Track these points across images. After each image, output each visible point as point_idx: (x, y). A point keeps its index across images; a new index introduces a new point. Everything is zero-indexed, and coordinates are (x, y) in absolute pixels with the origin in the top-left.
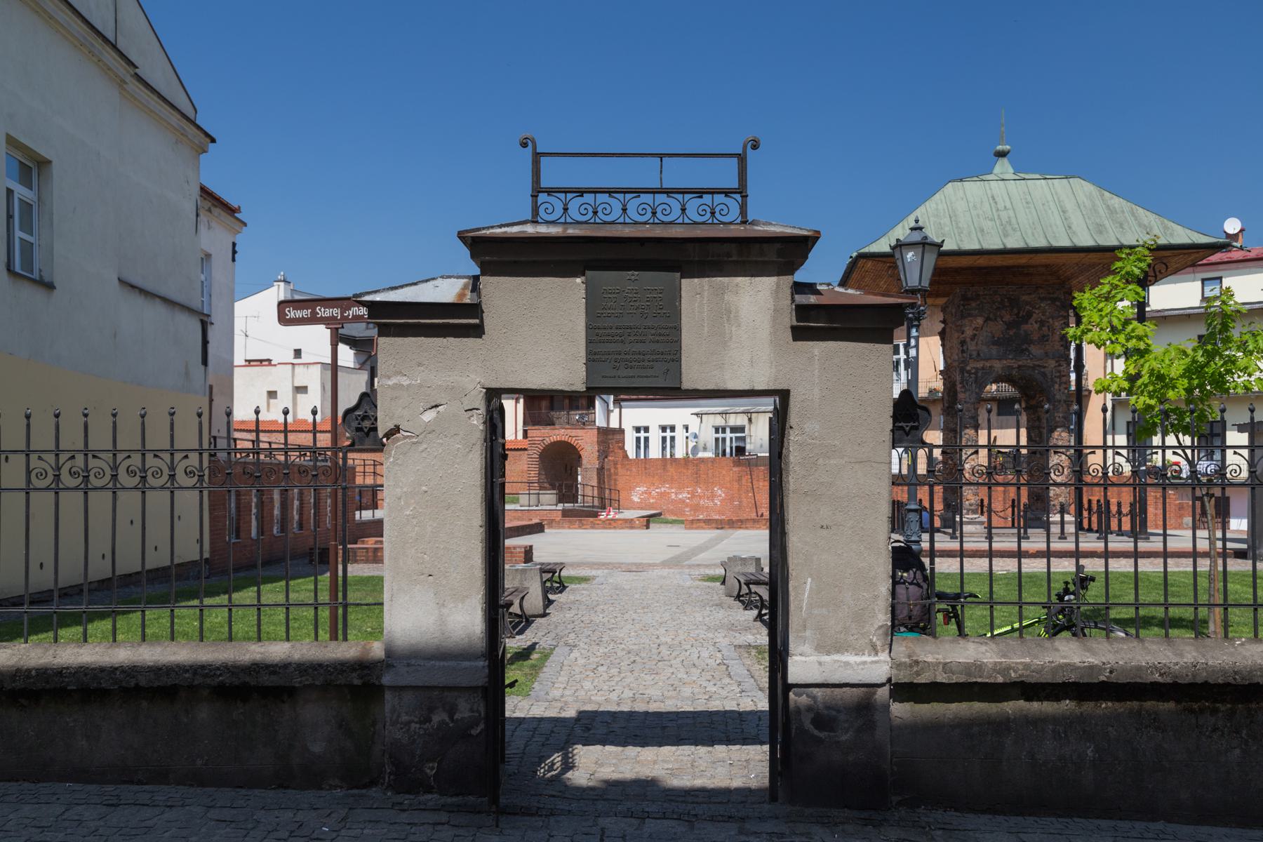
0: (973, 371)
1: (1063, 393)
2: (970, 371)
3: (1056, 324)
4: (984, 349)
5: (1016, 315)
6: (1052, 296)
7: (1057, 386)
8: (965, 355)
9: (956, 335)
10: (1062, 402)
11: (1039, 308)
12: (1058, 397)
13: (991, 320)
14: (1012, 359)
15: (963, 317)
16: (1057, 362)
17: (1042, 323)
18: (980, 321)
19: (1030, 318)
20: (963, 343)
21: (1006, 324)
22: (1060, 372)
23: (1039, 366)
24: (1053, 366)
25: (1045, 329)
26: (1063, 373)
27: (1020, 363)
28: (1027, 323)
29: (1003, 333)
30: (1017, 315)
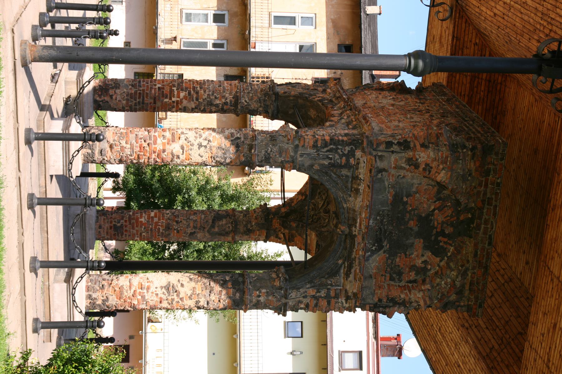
0: (352, 161)
1: (300, 302)
2: (354, 156)
3: (420, 295)
4: (388, 181)
5: (443, 231)
6: (467, 287)
7: (312, 292)
8: (382, 147)
9: (420, 132)
10: (284, 301)
11: (449, 267)
12: (293, 294)
13: (439, 192)
14: (367, 227)
15: (453, 148)
16: (355, 295)
17: (422, 271)
18: (442, 177)
19: (433, 253)
20: (405, 145)
21: (428, 216)
22: (337, 296)
23: (350, 267)
24: (348, 288)
25: (413, 275)
26: (333, 301)
27: (359, 239)
28: (426, 248)
29: (413, 210)
30: (442, 233)
